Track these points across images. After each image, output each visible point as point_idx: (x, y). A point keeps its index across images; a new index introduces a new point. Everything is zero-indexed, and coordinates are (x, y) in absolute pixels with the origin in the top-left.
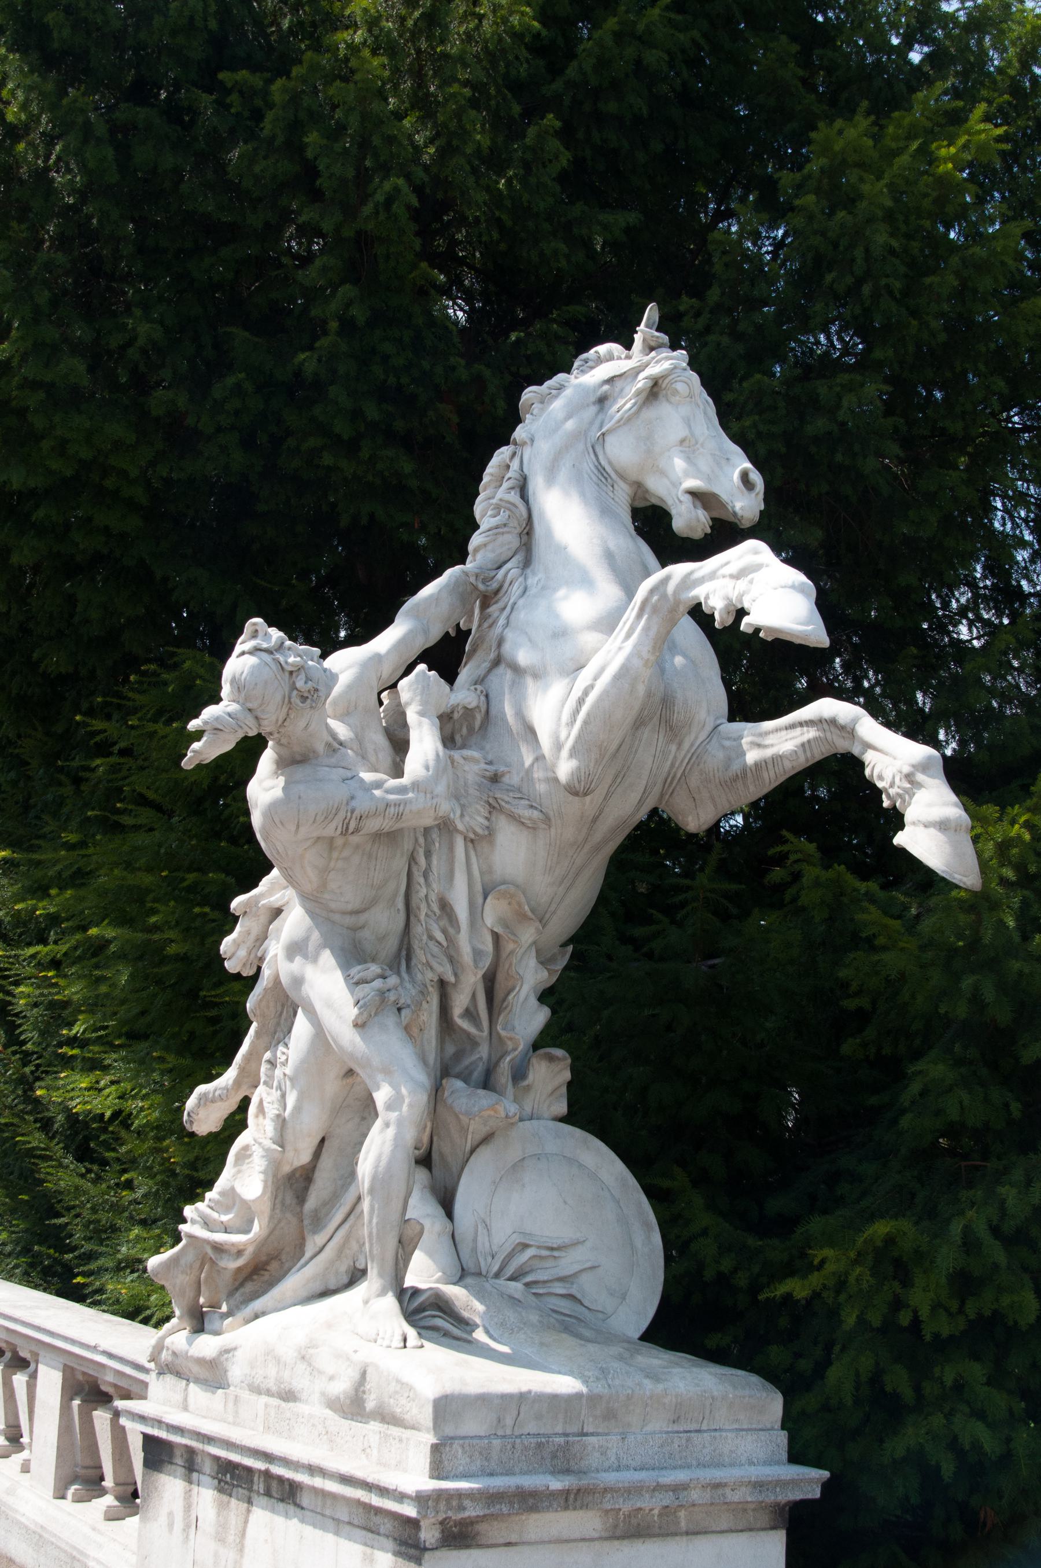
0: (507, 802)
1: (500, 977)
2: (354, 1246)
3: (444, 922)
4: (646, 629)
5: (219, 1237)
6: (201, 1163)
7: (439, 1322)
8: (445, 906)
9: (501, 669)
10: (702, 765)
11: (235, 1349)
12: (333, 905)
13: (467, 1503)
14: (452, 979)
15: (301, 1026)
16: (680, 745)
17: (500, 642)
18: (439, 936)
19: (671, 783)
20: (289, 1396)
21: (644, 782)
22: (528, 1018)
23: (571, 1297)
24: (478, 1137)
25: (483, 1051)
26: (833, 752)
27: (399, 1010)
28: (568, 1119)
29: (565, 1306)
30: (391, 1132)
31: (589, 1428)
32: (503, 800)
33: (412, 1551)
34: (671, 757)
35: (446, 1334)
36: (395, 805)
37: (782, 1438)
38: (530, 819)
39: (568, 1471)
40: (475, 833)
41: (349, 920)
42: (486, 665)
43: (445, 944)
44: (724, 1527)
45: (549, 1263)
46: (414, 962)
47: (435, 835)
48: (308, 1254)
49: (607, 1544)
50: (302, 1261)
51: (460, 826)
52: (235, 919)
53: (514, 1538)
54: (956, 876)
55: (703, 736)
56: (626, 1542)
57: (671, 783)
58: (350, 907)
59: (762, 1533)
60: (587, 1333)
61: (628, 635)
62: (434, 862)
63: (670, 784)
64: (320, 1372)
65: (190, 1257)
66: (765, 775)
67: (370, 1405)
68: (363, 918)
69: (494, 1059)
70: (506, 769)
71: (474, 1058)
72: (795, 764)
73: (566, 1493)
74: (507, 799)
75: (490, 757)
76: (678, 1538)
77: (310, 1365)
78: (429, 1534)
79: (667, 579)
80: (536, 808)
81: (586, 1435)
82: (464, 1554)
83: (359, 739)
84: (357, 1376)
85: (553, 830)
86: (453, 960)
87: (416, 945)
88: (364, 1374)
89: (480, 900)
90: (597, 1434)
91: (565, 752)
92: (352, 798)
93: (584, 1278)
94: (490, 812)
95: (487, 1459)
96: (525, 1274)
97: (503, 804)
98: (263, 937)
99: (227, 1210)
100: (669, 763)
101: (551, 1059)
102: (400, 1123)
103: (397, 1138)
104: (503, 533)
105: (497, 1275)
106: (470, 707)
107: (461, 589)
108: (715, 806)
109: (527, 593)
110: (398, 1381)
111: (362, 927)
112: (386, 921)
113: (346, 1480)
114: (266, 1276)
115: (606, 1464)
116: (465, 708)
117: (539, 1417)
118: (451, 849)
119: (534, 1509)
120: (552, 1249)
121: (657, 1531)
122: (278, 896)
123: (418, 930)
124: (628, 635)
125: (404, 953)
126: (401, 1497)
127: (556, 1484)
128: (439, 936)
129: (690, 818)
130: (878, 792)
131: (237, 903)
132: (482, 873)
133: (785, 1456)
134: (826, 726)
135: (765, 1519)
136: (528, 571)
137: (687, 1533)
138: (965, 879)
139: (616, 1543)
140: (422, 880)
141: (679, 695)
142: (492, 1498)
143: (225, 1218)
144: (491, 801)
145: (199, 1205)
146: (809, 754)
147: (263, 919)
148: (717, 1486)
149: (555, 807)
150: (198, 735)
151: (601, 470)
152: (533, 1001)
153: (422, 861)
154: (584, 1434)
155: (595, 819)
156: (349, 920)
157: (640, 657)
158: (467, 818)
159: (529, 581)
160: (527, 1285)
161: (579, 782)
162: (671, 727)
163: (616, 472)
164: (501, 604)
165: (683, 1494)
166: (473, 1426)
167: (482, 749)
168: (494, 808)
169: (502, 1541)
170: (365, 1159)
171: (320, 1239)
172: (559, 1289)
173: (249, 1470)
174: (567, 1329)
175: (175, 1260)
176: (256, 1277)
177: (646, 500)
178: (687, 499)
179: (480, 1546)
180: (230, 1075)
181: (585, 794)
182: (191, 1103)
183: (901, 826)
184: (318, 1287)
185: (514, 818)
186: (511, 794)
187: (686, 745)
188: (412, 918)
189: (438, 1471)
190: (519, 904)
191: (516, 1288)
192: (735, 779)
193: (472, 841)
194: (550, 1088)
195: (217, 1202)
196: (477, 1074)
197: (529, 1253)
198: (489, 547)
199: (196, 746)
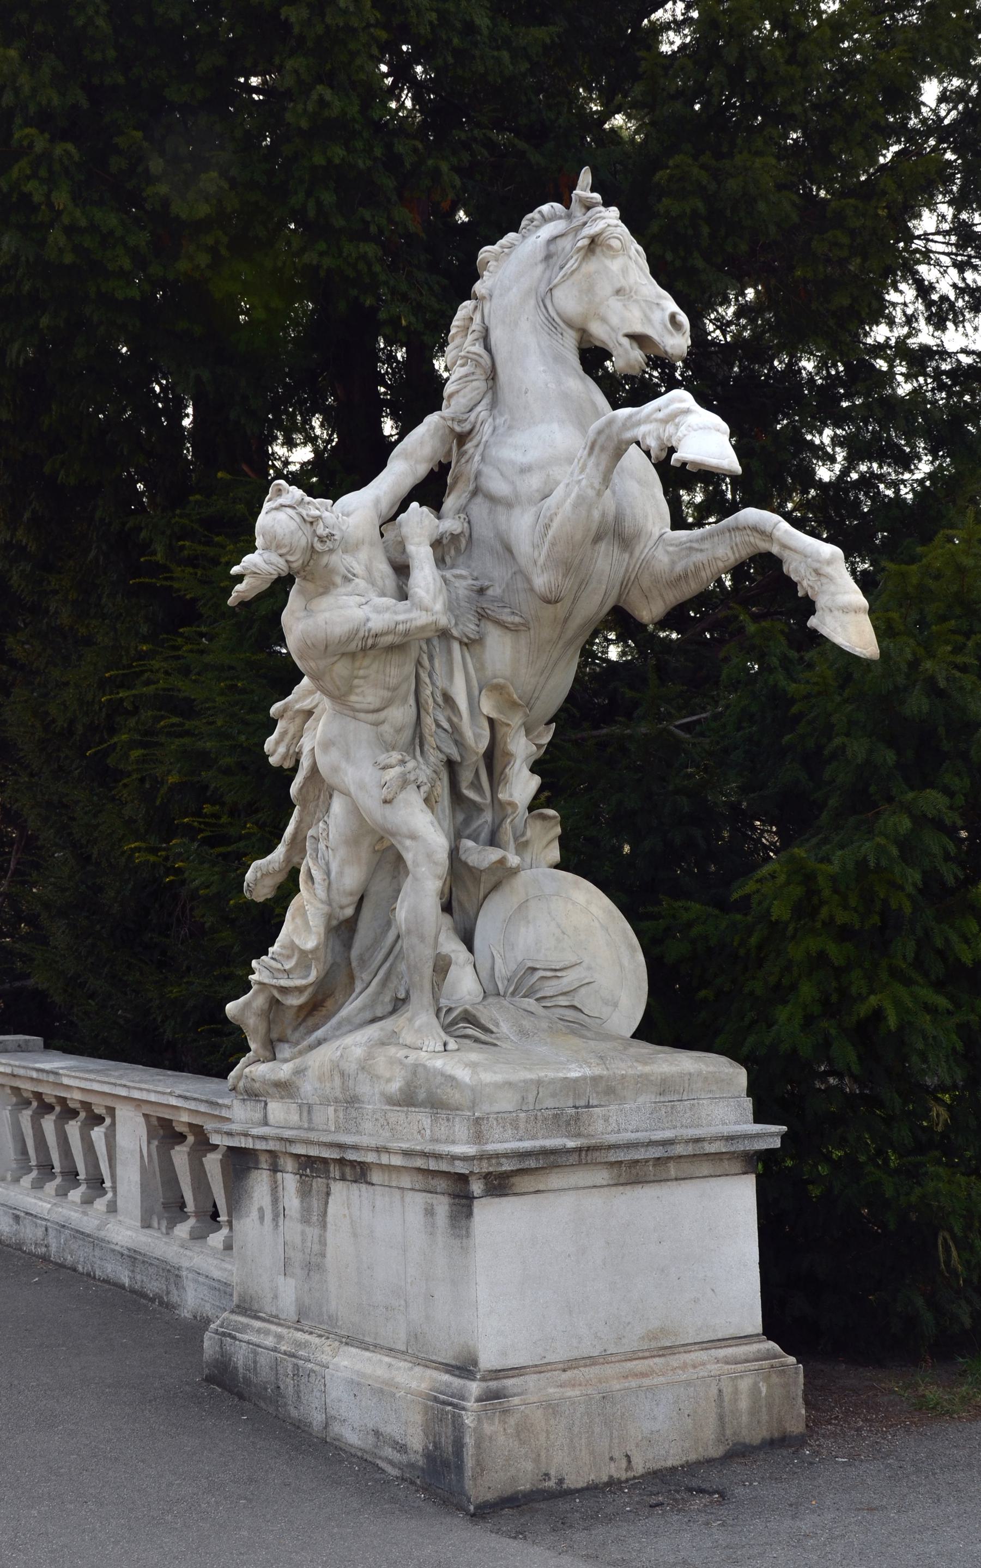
1: (498, 753)
2: (393, 978)
3: (449, 712)
5: (284, 982)
6: (265, 922)
7: (470, 1032)
8: (448, 700)
9: (479, 499)
11: (306, 1069)
12: (358, 706)
13: (503, 1160)
14: (459, 759)
15: (337, 806)
16: (631, 554)
17: (478, 475)
18: (446, 725)
19: (627, 585)
21: (604, 587)
22: (522, 785)
23: (574, 1007)
24: (489, 886)
25: (487, 816)
26: (757, 551)
27: (418, 787)
28: (562, 866)
29: (570, 1014)
31: (594, 1102)
33: (464, 1201)
34: (625, 564)
35: (477, 1040)
37: (748, 1103)
38: (513, 623)
39: (579, 1135)
40: (468, 638)
42: (466, 495)
43: (450, 730)
44: (706, 1173)
45: (554, 982)
46: (426, 747)
47: (436, 642)
48: (357, 990)
49: (614, 1189)
50: (354, 995)
51: (455, 633)
52: (275, 722)
53: (541, 1187)
54: (857, 649)
55: (651, 543)
56: (628, 1187)
57: (627, 585)
58: (372, 707)
59: (736, 1177)
60: (588, 1034)
63: (624, 587)
64: (378, 1077)
66: (703, 574)
67: (422, 1095)
68: (382, 715)
69: (497, 822)
70: (490, 583)
71: (480, 822)
72: (726, 563)
73: (579, 1150)
74: (492, 608)
75: (475, 574)
76: (669, 1183)
77: (369, 1073)
78: (477, 1187)
80: (517, 614)
81: (593, 1107)
82: (504, 1200)
83: (369, 570)
85: (532, 632)
86: (459, 743)
87: (426, 732)
89: (477, 693)
90: (601, 1106)
92: (368, 620)
93: (583, 991)
94: (479, 620)
95: (517, 1128)
96: (536, 991)
97: (489, 612)
98: (299, 735)
99: (289, 957)
100: (624, 568)
101: (544, 818)
104: (472, 381)
105: (513, 994)
106: (455, 533)
107: (440, 433)
108: (664, 601)
109: (496, 433)
110: (443, 1074)
111: (383, 722)
112: (402, 714)
114: (324, 1011)
115: (609, 1129)
116: (452, 534)
117: (554, 1095)
118: (449, 652)
120: (556, 970)
121: (652, 1178)
122: (309, 700)
123: (428, 721)
125: (417, 741)
127: (571, 1144)
128: (446, 725)
129: (644, 613)
130: (794, 585)
131: (275, 709)
132: (476, 670)
133: (751, 1117)
134: (749, 532)
136: (495, 412)
137: (676, 1179)
138: (864, 651)
139: (621, 1188)
140: (427, 680)
141: (628, 511)
144: (479, 610)
145: (263, 957)
146: (737, 555)
147: (298, 721)
148: (698, 1140)
149: (533, 612)
150: (239, 578)
151: (551, 321)
152: (526, 772)
153: (426, 662)
154: (588, 1106)
155: (566, 620)
158: (461, 627)
159: (498, 421)
160: (537, 1000)
161: (551, 593)
162: (623, 539)
163: (564, 321)
164: (474, 442)
165: (669, 1148)
167: (469, 567)
168: (482, 616)
169: (532, 1190)
170: (401, 908)
171: (366, 976)
172: (563, 1001)
173: (325, 1161)
174: (574, 1032)
175: (247, 1004)
177: (590, 342)
178: (626, 342)
179: (515, 1194)
180: (280, 852)
181: (557, 602)
182: (249, 876)
183: (813, 612)
184: (368, 1015)
186: (496, 604)
187: (637, 553)
188: (423, 713)
190: (509, 695)
191: (530, 1003)
192: (679, 578)
193: (466, 644)
194: (544, 842)
195: (280, 954)
196: (484, 835)
198: (461, 393)
199: (238, 587)
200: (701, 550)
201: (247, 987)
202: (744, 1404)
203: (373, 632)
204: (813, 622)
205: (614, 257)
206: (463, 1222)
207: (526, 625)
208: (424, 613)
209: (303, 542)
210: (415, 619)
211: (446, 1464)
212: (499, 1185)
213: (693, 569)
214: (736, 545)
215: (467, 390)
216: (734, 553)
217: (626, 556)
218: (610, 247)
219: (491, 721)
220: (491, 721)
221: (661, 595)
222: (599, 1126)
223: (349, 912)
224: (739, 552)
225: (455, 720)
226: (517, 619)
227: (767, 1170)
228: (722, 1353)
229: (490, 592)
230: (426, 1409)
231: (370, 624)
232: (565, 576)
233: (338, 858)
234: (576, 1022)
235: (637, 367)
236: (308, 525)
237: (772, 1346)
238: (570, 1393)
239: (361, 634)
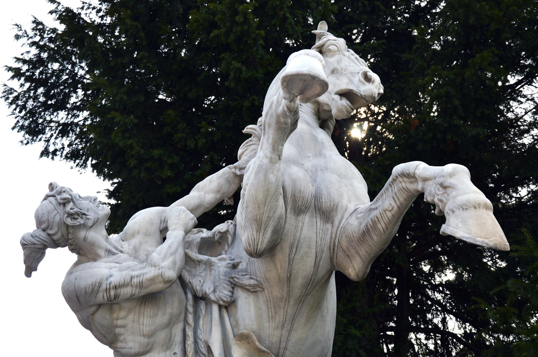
0: (238, 278)
10: (346, 232)
16: (332, 224)
19: (334, 250)
21: (314, 251)
32: (236, 278)
34: (329, 233)
36: (137, 277)
38: (250, 286)
51: (212, 297)
54: (478, 239)
57: (334, 250)
62: (201, 323)
63: (333, 249)
70: (240, 260)
72: (393, 212)
74: (237, 276)
80: (254, 279)
85: (266, 291)
92: (111, 276)
94: (233, 288)
97: (236, 280)
100: (329, 236)
104: (251, 145)
106: (222, 231)
107: (226, 176)
108: (360, 257)
129: (350, 270)
134: (400, 179)
138: (486, 241)
141: (324, 191)
144: (231, 280)
146: (398, 203)
149: (263, 275)
157: (267, 157)
158: (218, 293)
161: (250, 246)
162: (323, 212)
168: (234, 285)
185: (243, 287)
186: (240, 273)
187: (336, 223)
198: (245, 154)
200: (377, 208)
203: (112, 284)
204: (446, 229)
205: (332, 56)
208: (153, 268)
209: (58, 218)
210: (146, 273)
213: (371, 224)
214: (396, 194)
215: (248, 151)
216: (395, 202)
217: (329, 226)
218: (330, 50)
221: (357, 253)
224: (399, 199)
226: (252, 282)
229: (240, 267)
231: (111, 279)
232: (258, 231)
235: (345, 111)
236: (62, 206)
239: (104, 287)
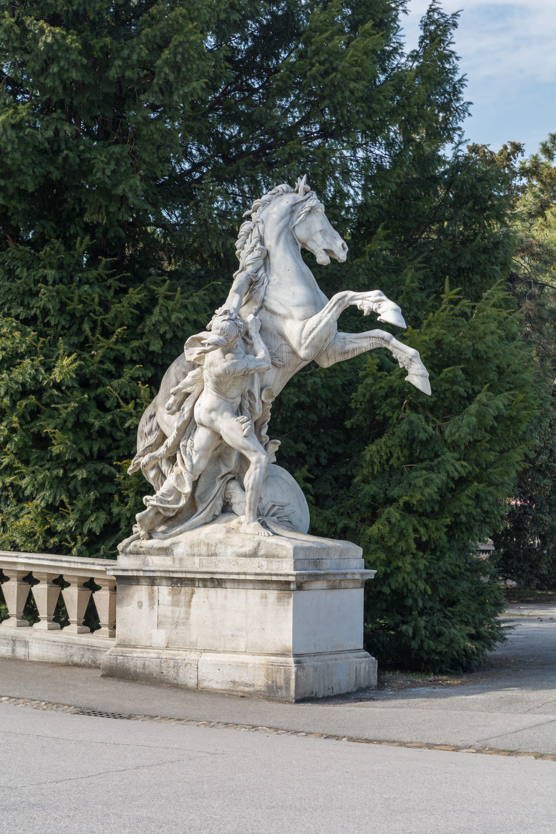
4: (336, 311)
8: (251, 394)
20: (215, 554)
30: (258, 470)
41: (231, 401)
48: (200, 510)
61: (329, 312)
65: (152, 514)
67: (261, 552)
79: (345, 296)
84: (256, 545)
88: (259, 544)
91: (303, 347)
101: (275, 443)
102: (261, 468)
103: (260, 472)
113: (256, 574)
119: (317, 580)
124: (329, 312)
126: (288, 575)
127: (322, 572)
135: (359, 585)
142: (310, 575)
143: (169, 499)
147: (182, 397)
148: (354, 574)
156: (231, 401)
166: (301, 556)
175: (146, 514)
176: (174, 519)
184: (203, 522)
189: (295, 569)
191: (275, 518)
197: (276, 508)
201: (145, 508)
202: (362, 672)
206: (286, 600)
207: (284, 366)
211: (280, 688)
212: (300, 587)
219: (263, 402)
220: (263, 402)
222: (324, 566)
223: (196, 478)
225: (252, 402)
227: (368, 585)
228: (354, 654)
230: (267, 669)
233: (198, 455)
234: (292, 526)
237: (367, 653)
238: (319, 664)
